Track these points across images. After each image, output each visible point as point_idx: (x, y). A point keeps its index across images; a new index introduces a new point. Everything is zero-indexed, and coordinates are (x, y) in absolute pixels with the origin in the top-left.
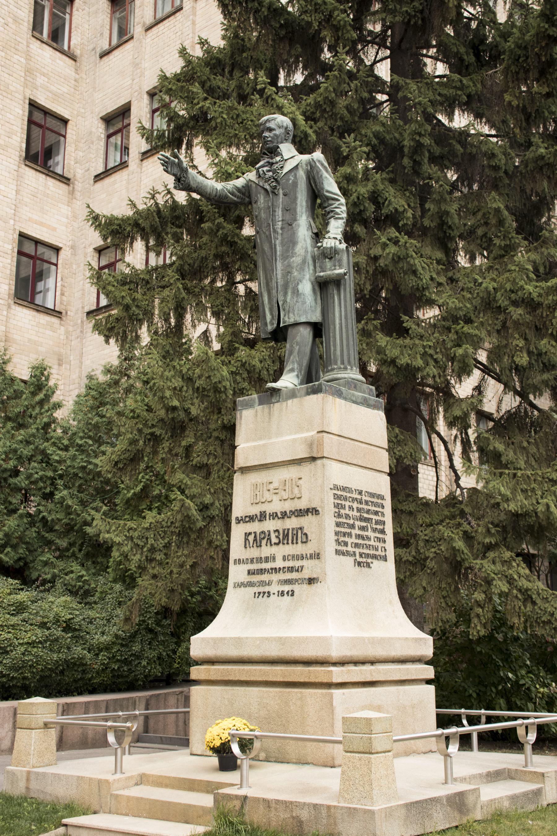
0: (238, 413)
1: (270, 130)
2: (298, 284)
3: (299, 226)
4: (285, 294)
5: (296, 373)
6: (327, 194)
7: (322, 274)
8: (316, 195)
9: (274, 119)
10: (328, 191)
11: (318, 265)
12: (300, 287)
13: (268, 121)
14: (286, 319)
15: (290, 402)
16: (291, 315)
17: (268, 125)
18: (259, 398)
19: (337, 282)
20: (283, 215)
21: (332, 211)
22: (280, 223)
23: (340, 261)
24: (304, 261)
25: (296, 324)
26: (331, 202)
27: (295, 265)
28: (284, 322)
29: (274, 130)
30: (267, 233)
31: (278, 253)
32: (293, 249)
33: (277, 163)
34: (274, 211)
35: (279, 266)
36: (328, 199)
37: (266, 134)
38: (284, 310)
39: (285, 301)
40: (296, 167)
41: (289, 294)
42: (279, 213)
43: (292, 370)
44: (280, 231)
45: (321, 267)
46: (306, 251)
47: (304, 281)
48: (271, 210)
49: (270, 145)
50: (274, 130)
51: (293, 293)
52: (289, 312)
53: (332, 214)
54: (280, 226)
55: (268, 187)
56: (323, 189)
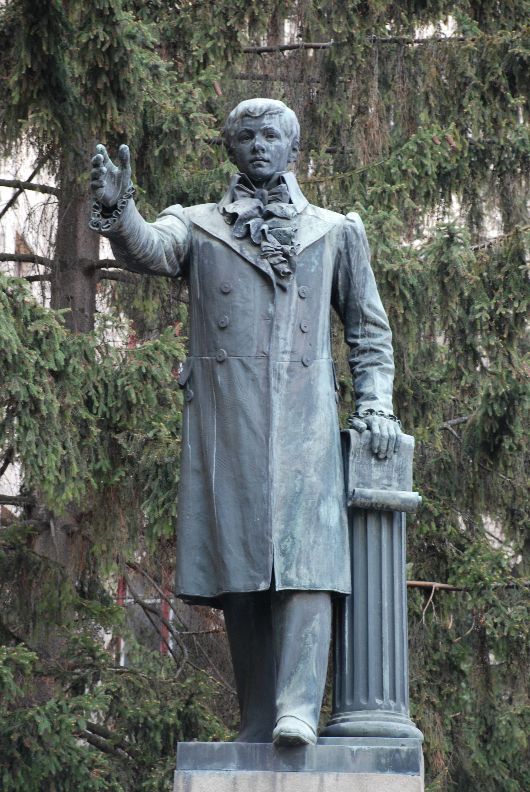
0: (179, 776)
1: (270, 134)
2: (319, 503)
3: (318, 370)
4: (289, 519)
5: (312, 706)
6: (368, 311)
7: (368, 491)
8: (345, 309)
9: (279, 113)
10: (369, 306)
11: (352, 467)
12: (323, 510)
13: (267, 112)
14: (292, 575)
15: (330, 778)
16: (303, 570)
17: (266, 121)
18: (242, 753)
19: (386, 512)
20: (294, 342)
21: (373, 350)
22: (287, 357)
23: (400, 470)
24: (329, 454)
25: (312, 592)
26: (370, 328)
27: (313, 458)
28: (285, 582)
29: (278, 137)
30: (259, 372)
31: (276, 422)
32: (308, 422)
33: (286, 218)
34: (278, 328)
35: (278, 453)
36: (367, 320)
37: (260, 141)
38: (283, 553)
39: (288, 535)
40: (322, 240)
41: (300, 520)
42: (286, 334)
43: (306, 698)
44: (285, 376)
45: (359, 473)
46: (332, 431)
47: (330, 499)
48: (271, 322)
49: (266, 170)
50: (278, 137)
51: (309, 521)
52: (298, 562)
53: (374, 358)
54: (286, 365)
55: (270, 271)
56: (362, 298)
